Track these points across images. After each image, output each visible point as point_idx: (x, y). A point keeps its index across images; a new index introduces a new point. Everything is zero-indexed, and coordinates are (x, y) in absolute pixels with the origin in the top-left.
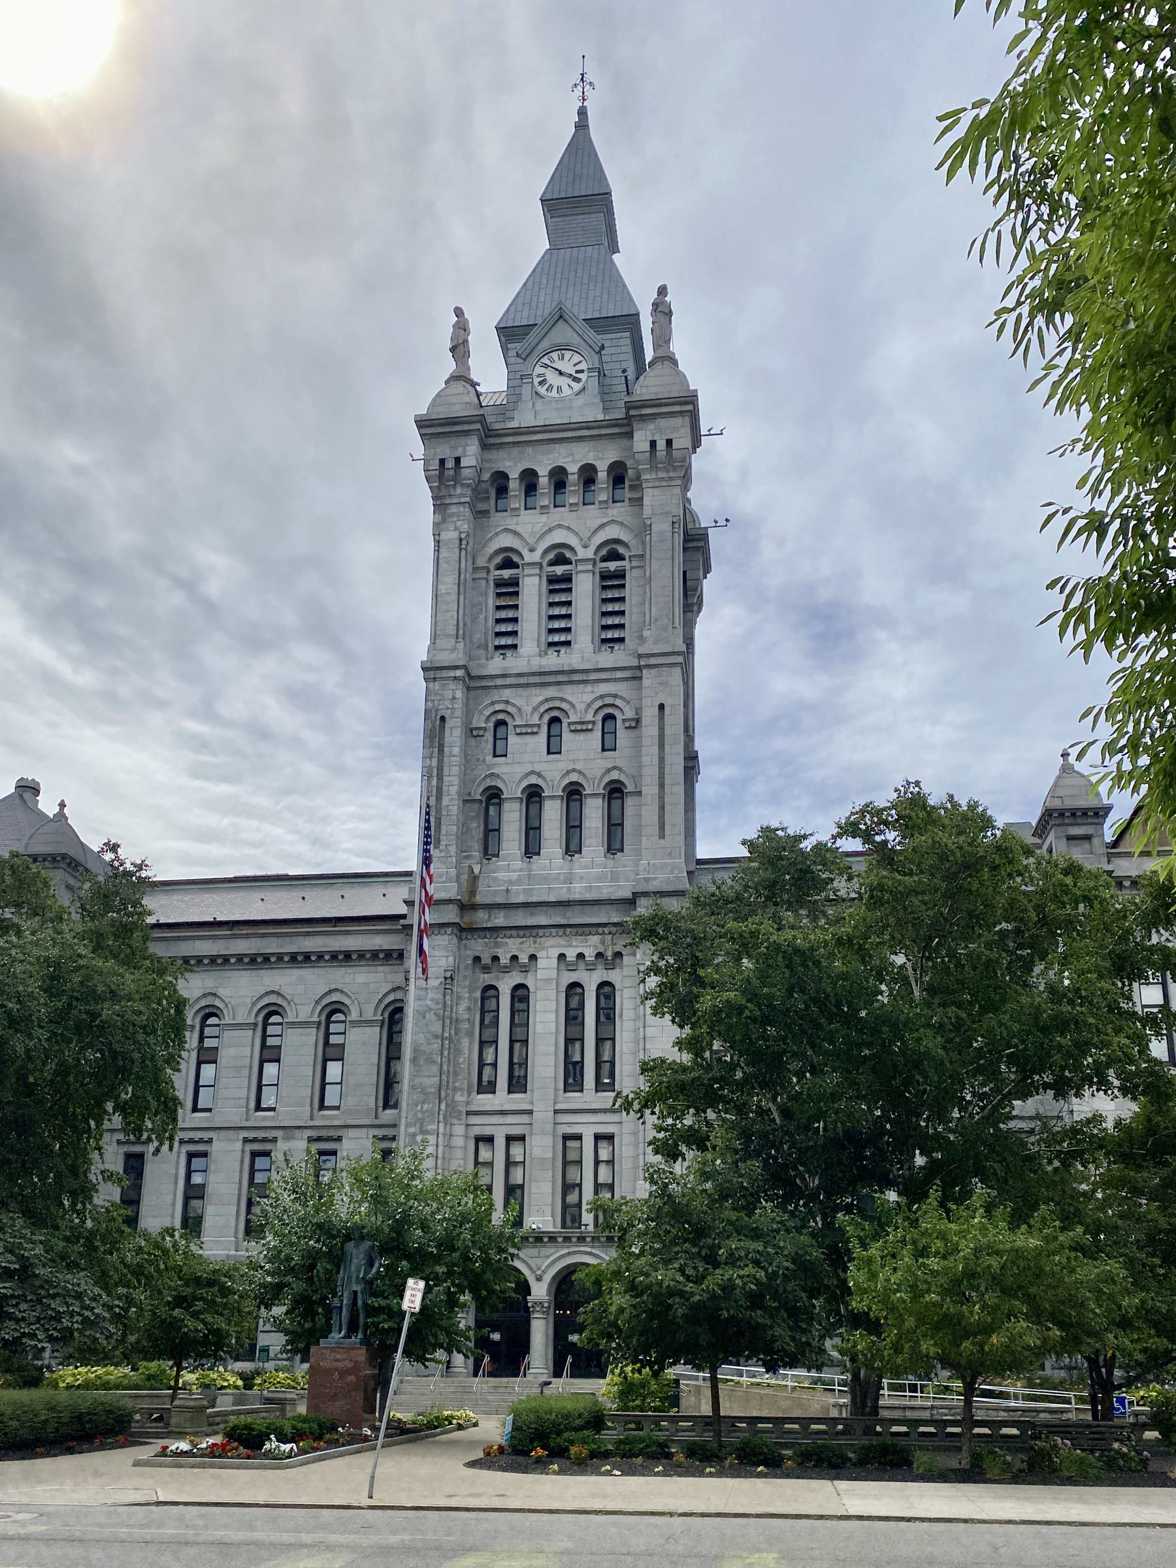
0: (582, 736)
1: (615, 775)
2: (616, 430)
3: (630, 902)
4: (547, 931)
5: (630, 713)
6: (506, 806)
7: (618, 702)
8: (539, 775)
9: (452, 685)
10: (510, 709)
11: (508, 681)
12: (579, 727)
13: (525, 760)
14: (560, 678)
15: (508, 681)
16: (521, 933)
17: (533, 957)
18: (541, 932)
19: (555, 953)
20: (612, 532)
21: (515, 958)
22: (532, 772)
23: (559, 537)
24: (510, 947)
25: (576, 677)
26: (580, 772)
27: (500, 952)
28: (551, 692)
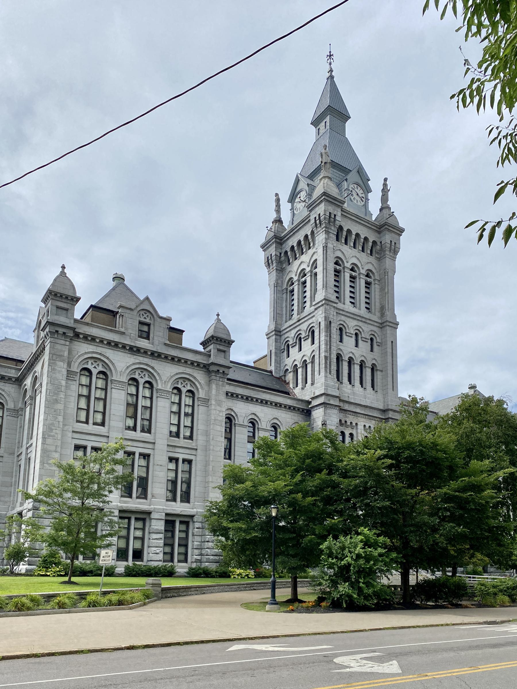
0: (365, 343)
1: (374, 362)
2: (375, 228)
3: (384, 411)
4: (361, 415)
8: (353, 354)
9: (333, 309)
10: (345, 324)
11: (344, 313)
12: (365, 340)
13: (348, 347)
14: (359, 318)
15: (344, 313)
16: (353, 414)
17: (356, 424)
18: (359, 415)
19: (363, 424)
21: (351, 423)
22: (351, 352)
23: (355, 261)
24: (350, 418)
25: (363, 320)
26: (365, 357)
27: (347, 420)
28: (360, 324)
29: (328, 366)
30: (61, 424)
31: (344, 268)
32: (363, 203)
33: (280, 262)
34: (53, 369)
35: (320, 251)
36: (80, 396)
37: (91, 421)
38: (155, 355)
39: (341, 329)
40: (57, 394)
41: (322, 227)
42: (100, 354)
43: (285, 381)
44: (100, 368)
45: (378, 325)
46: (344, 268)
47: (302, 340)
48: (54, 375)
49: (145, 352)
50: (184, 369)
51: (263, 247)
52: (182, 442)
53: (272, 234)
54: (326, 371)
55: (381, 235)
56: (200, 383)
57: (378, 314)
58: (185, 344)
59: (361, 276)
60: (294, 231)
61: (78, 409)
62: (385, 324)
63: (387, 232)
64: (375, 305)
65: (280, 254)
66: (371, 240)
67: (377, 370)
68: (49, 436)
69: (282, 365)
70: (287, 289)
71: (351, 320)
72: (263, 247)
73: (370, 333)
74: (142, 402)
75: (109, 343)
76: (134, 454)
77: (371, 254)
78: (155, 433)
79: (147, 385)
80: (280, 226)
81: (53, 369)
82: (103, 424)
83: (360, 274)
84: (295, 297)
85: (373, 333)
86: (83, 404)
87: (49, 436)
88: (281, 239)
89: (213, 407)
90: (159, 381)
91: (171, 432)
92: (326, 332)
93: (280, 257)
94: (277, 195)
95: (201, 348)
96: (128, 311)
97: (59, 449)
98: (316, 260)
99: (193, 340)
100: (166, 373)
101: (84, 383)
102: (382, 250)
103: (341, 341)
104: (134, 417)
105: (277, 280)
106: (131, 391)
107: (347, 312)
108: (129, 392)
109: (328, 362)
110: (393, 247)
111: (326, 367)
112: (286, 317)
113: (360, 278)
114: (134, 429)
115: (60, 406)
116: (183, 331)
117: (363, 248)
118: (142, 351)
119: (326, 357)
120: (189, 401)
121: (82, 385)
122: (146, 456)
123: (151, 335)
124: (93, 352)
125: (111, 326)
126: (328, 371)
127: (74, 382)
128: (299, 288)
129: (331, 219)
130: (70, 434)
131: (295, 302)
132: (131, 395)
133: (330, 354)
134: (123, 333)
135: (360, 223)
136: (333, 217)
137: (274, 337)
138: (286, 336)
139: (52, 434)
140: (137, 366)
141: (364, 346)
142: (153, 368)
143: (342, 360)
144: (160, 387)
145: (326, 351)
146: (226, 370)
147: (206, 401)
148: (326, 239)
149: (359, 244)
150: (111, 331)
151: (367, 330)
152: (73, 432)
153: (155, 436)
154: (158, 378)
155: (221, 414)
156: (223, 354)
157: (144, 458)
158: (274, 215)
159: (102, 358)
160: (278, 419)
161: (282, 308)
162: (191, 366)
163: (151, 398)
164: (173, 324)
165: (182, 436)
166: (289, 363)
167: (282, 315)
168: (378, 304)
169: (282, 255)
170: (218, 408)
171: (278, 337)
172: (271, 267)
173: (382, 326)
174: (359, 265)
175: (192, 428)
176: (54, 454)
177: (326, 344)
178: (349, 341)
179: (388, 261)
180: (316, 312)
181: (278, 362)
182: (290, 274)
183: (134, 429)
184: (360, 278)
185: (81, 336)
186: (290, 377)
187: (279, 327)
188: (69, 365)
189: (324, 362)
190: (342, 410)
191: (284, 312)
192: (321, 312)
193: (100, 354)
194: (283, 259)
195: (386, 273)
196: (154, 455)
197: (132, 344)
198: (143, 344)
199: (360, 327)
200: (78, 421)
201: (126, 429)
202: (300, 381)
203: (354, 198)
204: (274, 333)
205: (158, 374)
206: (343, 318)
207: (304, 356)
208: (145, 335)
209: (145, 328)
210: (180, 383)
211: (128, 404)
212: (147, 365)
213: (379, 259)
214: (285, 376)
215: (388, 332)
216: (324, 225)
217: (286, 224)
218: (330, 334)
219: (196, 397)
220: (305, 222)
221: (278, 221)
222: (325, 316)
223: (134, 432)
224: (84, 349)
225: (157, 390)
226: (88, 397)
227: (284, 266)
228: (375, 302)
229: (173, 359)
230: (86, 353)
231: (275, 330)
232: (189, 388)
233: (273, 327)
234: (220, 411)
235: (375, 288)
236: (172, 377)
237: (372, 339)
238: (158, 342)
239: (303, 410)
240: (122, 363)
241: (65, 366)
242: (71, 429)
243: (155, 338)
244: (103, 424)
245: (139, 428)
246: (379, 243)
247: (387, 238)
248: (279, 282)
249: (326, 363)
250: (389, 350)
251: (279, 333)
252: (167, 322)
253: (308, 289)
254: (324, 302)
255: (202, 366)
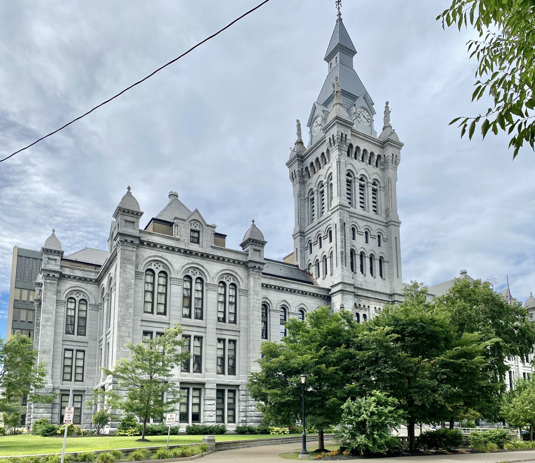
1: (382, 255)
3: (391, 295)
5: (385, 237)
6: (366, 258)
7: (382, 232)
8: (364, 249)
9: (346, 213)
10: (356, 225)
11: (355, 216)
13: (359, 244)
14: (368, 219)
15: (355, 216)
17: (369, 307)
19: (374, 306)
20: (376, 177)
21: (364, 306)
22: (363, 248)
24: (363, 302)
28: (369, 224)
29: (344, 260)
30: (132, 314)
31: (354, 179)
32: (369, 124)
33: (302, 176)
34: (124, 271)
35: (335, 165)
36: (146, 291)
37: (155, 312)
38: (204, 256)
39: (353, 229)
40: (127, 291)
41: (336, 145)
42: (161, 257)
43: (309, 273)
44: (161, 269)
45: (384, 224)
46: (354, 179)
47: (322, 239)
48: (125, 276)
49: (197, 254)
50: (227, 266)
51: (287, 164)
52: (228, 326)
53: (295, 154)
54: (342, 264)
55: (385, 149)
56: (240, 278)
57: (384, 215)
58: (227, 247)
59: (369, 185)
60: (313, 149)
61: (145, 302)
62: (390, 223)
63: (389, 147)
64: (381, 208)
65: (302, 169)
66: (376, 154)
67: (384, 261)
68: (123, 324)
69: (307, 260)
70: (308, 198)
71: (362, 221)
72: (287, 164)
73: (378, 231)
74: (195, 295)
75: (168, 248)
76: (190, 336)
77: (377, 166)
78: (206, 319)
79: (199, 281)
80: (301, 147)
81: (124, 271)
82: (165, 314)
83: (367, 183)
84: (315, 204)
85: (380, 231)
86: (149, 298)
87: (123, 324)
88: (302, 157)
89: (252, 296)
90: (208, 277)
91: (219, 318)
92: (341, 232)
93: (302, 172)
94: (298, 121)
95: (240, 249)
96: (182, 222)
97: (131, 335)
98: (331, 173)
99: (233, 242)
100: (213, 270)
101: (149, 281)
102: (386, 162)
103: (354, 239)
104: (190, 307)
105: (300, 191)
106: (187, 286)
107: (358, 215)
108: (185, 287)
109: (344, 256)
110: (394, 160)
111: (342, 260)
112: (308, 221)
113: (367, 187)
114: (190, 316)
115: (131, 301)
116: (226, 236)
117: (370, 161)
118: (194, 253)
119: (342, 253)
120: (232, 292)
121: (148, 283)
122: (199, 338)
123: (201, 240)
124: (155, 256)
125: (169, 234)
126: (344, 264)
127: (141, 281)
128: (318, 197)
129: (343, 138)
130: (139, 323)
131: (315, 208)
132: (187, 289)
133: (345, 250)
134: (178, 240)
135: (367, 141)
136: (344, 136)
137: (299, 237)
138: (309, 236)
139: (125, 323)
140: (191, 266)
141: (373, 242)
142: (203, 267)
143: (355, 254)
144: (208, 282)
145: (342, 248)
146: (261, 266)
147: (246, 292)
148: (339, 155)
149: (366, 158)
150: (169, 238)
151: (375, 229)
152: (142, 320)
153: (206, 322)
154: (207, 274)
155: (258, 302)
156: (258, 253)
157: (199, 340)
158: (296, 138)
159: (163, 260)
160: (304, 305)
161: (305, 214)
162: (233, 264)
163: (202, 291)
164: (217, 231)
165: (227, 321)
166: (311, 258)
167: (305, 219)
168: (383, 207)
169: (304, 170)
170: (256, 297)
171: (302, 238)
172: (295, 181)
173: (387, 225)
174: (367, 176)
175: (235, 314)
176: (128, 338)
177: (342, 242)
178: (360, 239)
179: (390, 171)
180: (333, 215)
181: (303, 258)
182: (310, 186)
183: (190, 316)
184: (367, 187)
185: (145, 243)
186: (313, 270)
187: (303, 229)
188: (137, 267)
189: (340, 256)
190: (356, 296)
191: (307, 217)
192: (336, 216)
193: (161, 257)
194: (304, 173)
195: (389, 181)
196: (206, 337)
197: (186, 248)
198: (194, 247)
199: (369, 227)
200: (145, 312)
201: (183, 317)
202: (321, 273)
203: (361, 120)
204: (299, 234)
205: (207, 271)
206: (355, 220)
207: (324, 252)
208: (196, 240)
209: (196, 235)
210: (224, 278)
211: (184, 297)
212: (198, 264)
213: (383, 170)
214: (309, 269)
215: (392, 230)
216: (337, 144)
217: (306, 144)
218: (345, 234)
219: (238, 289)
220: (321, 142)
221: (300, 143)
222: (340, 219)
223: (189, 319)
224: (148, 253)
225: (206, 284)
226: (153, 293)
227: (306, 179)
228: (381, 206)
229: (218, 258)
230: (149, 257)
231: (300, 232)
232: (232, 281)
233: (298, 230)
234: (258, 300)
235: (381, 195)
236: (218, 273)
237: (379, 236)
238: (206, 245)
239: (325, 296)
240: (178, 264)
241: (134, 268)
242: (140, 319)
243: (204, 242)
244: (165, 314)
245: (193, 316)
246: (383, 157)
247: (390, 151)
248: (302, 192)
249: (342, 257)
250: (394, 245)
251: (303, 234)
252: (213, 229)
253: (325, 197)
254: (338, 207)
255: (242, 263)
